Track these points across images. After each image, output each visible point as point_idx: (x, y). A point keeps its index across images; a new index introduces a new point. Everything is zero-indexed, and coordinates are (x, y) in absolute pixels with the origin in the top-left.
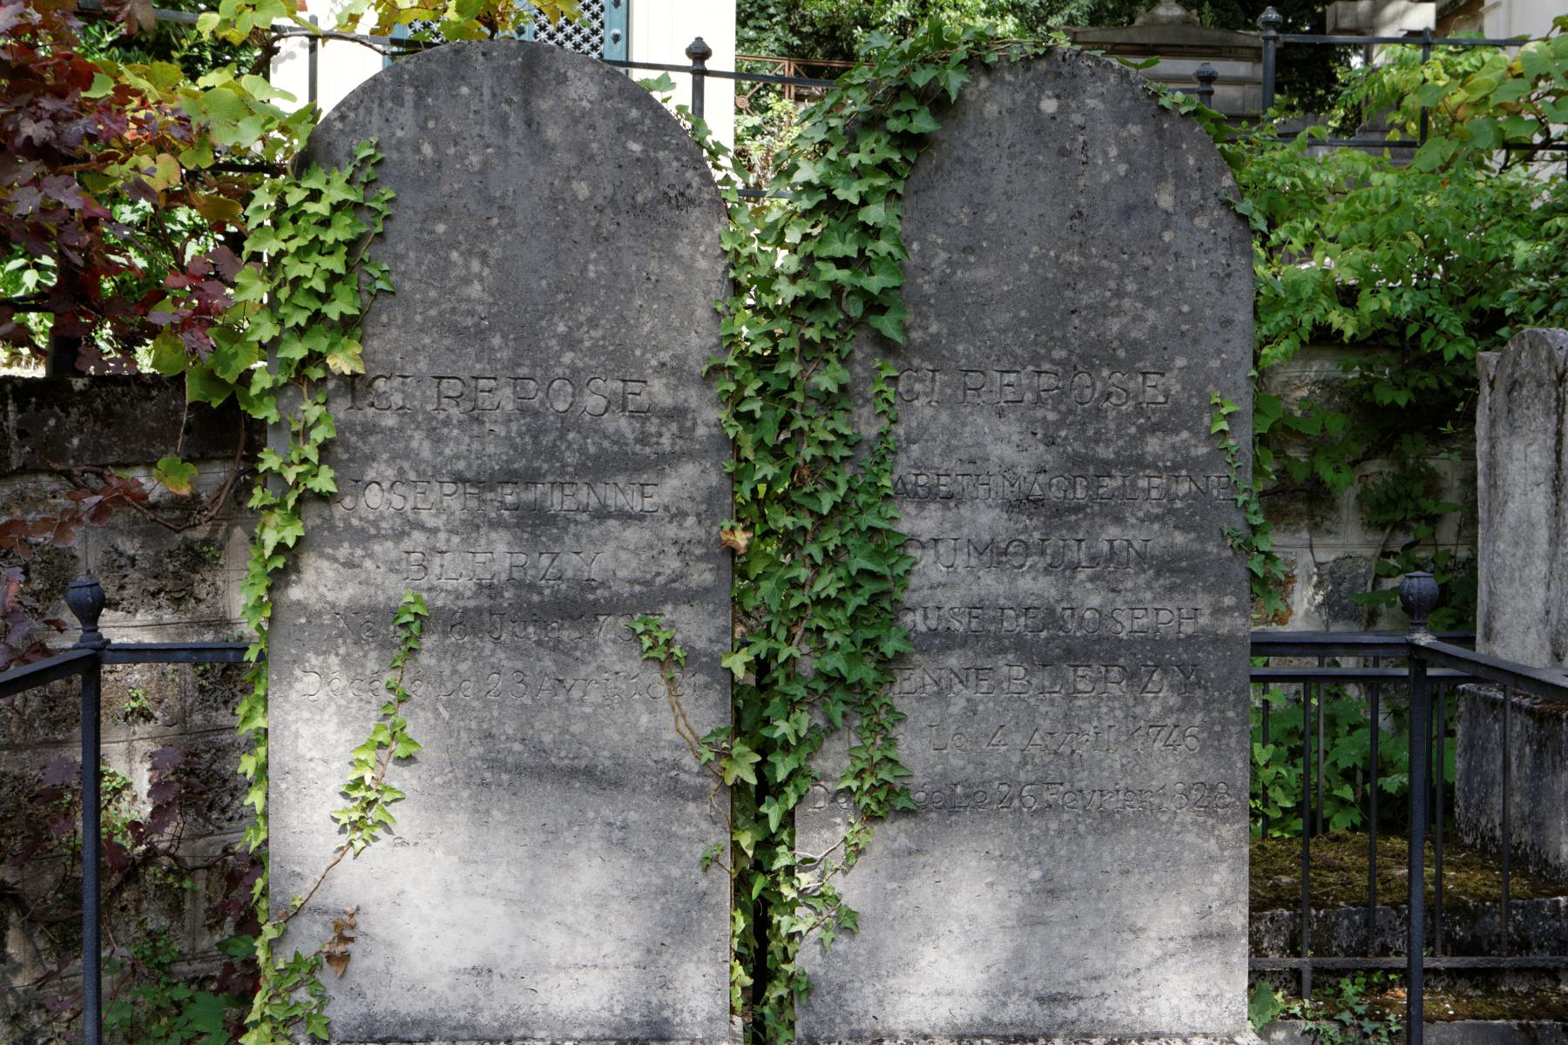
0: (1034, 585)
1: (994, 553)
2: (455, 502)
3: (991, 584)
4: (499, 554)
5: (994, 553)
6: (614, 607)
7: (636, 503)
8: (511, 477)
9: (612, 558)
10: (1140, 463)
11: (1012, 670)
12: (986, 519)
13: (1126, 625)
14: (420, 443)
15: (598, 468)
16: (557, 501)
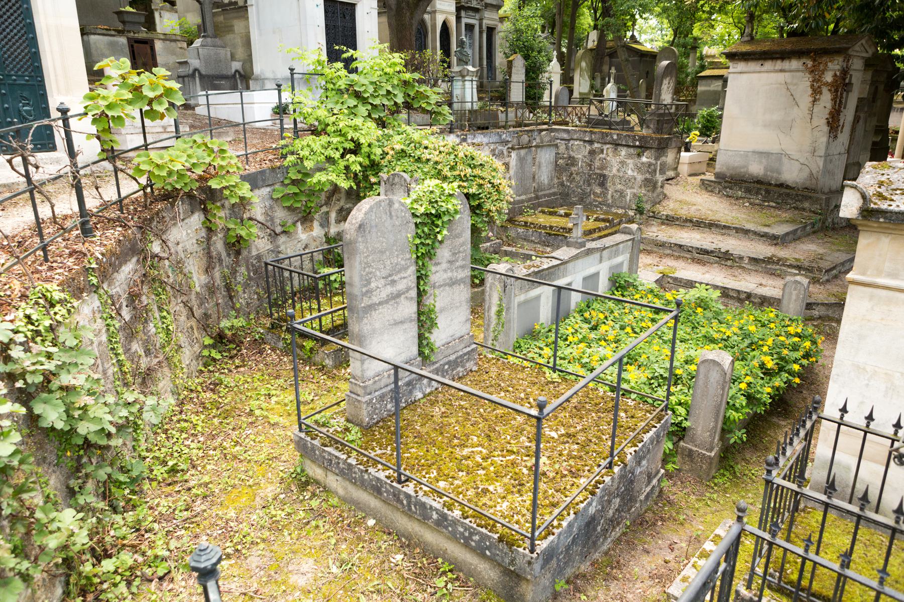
0: (450, 274)
1: (445, 271)
2: (383, 281)
3: (445, 276)
4: (389, 290)
5: (445, 271)
6: (404, 293)
7: (405, 275)
8: (390, 275)
9: (401, 286)
10: (459, 252)
11: (447, 288)
12: (444, 266)
13: (459, 277)
14: (378, 273)
15: (399, 272)
16: (396, 278)
